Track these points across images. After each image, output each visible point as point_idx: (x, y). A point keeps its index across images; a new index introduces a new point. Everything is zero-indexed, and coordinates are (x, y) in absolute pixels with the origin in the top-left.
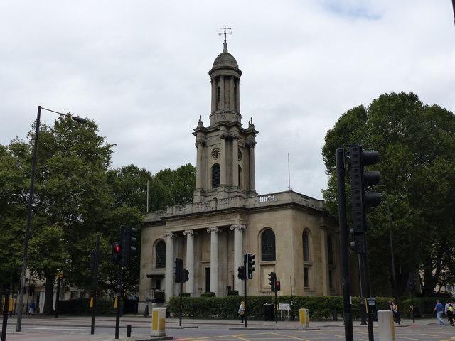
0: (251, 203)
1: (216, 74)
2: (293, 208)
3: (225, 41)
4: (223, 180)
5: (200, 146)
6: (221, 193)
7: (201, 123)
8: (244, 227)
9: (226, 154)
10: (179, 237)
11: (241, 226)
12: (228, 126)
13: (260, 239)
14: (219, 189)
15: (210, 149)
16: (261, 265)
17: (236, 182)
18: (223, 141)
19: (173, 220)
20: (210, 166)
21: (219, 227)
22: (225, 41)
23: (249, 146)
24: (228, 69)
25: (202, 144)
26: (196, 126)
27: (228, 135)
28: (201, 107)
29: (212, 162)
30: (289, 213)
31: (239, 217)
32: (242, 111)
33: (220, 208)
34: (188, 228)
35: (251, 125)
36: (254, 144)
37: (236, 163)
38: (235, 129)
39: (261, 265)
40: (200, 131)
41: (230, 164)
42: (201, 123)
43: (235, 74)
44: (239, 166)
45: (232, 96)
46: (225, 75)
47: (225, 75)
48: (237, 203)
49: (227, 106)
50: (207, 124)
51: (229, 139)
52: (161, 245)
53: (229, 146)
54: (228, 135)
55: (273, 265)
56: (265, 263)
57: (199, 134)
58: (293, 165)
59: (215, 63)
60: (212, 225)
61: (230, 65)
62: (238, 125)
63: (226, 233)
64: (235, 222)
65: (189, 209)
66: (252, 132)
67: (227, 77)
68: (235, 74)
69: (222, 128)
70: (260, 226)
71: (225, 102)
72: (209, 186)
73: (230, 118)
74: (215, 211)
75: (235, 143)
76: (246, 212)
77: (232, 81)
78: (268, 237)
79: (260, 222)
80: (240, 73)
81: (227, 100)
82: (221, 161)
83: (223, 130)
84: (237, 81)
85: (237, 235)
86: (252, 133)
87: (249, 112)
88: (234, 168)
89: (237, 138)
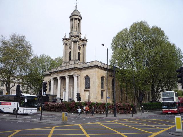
1: (72, 18)
3: (76, 6)
4: (72, 58)
5: (65, 45)
6: (72, 62)
8: (78, 75)
10: (56, 80)
13: (85, 80)
14: (70, 61)
16: (85, 91)
17: (77, 58)
18: (73, 43)
19: (53, 73)
20: (68, 52)
21: (69, 76)
22: (76, 6)
27: (75, 41)
32: (81, 32)
33: (69, 68)
36: (86, 45)
38: (78, 38)
39: (85, 91)
41: (75, 51)
43: (80, 18)
44: (79, 53)
46: (76, 18)
47: (76, 18)
50: (68, 37)
52: (50, 82)
53: (75, 45)
54: (75, 41)
55: (89, 90)
58: (99, 51)
60: (66, 75)
61: (77, 14)
63: (72, 78)
64: (75, 73)
65: (60, 69)
67: (76, 19)
68: (80, 18)
69: (73, 37)
70: (84, 75)
71: (75, 28)
72: (68, 60)
73: (75, 34)
75: (77, 43)
77: (78, 20)
78: (87, 78)
80: (81, 18)
81: (76, 27)
84: (80, 20)
85: (76, 78)
88: (77, 53)
89: (78, 42)
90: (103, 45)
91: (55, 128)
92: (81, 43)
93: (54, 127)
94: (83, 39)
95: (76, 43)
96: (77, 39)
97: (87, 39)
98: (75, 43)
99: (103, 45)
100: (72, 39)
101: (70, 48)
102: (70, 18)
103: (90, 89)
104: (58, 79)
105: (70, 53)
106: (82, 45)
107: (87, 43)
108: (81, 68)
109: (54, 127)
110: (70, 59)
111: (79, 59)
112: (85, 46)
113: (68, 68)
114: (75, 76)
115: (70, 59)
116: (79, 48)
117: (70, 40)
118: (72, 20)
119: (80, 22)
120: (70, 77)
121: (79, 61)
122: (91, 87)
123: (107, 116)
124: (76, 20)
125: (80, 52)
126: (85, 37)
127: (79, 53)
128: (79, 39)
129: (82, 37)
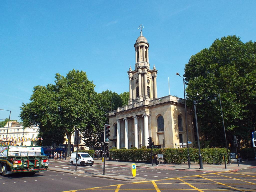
1: (137, 46)
10: (122, 121)
17: (146, 94)
37: (147, 85)
39: (158, 134)
43: (147, 46)
44: (148, 87)
53: (143, 78)
55: (163, 133)
56: (159, 132)
60: (134, 115)
67: (142, 47)
68: (147, 46)
70: (156, 114)
77: (144, 48)
90: (178, 74)
91: (121, 187)
93: (119, 186)
95: (144, 75)
99: (178, 74)
102: (135, 46)
103: (165, 132)
108: (152, 106)
109: (119, 186)
111: (149, 95)
122: (166, 128)
123: (189, 167)
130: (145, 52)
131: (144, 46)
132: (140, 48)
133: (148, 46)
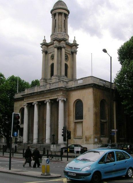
0: (72, 85)
1: (54, 12)
2: (92, 87)
4: (55, 73)
5: (44, 53)
6: (54, 79)
7: (45, 40)
8: (65, 99)
9: (58, 57)
10: (31, 106)
11: (62, 99)
12: (59, 41)
14: (53, 78)
15: (50, 55)
17: (63, 73)
18: (56, 50)
20: (50, 64)
23: (74, 53)
24: (60, 9)
25: (45, 52)
26: (42, 42)
28: (46, 33)
29: (51, 62)
30: (90, 91)
31: (61, 93)
34: (35, 101)
35: (75, 41)
36: (76, 52)
37: (64, 62)
38: (63, 42)
40: (45, 45)
42: (45, 40)
45: (63, 25)
48: (61, 85)
49: (60, 30)
50: (49, 41)
51: (59, 48)
52: (22, 110)
53: (59, 52)
55: (82, 122)
57: (44, 46)
59: (55, 6)
61: (61, 7)
62: (65, 40)
63: (55, 103)
66: (75, 45)
67: (60, 14)
69: (55, 42)
73: (60, 37)
74: (49, 90)
75: (63, 50)
76: (67, 91)
77: (63, 15)
78: (79, 104)
79: (75, 96)
82: (55, 61)
83: (56, 43)
84: (66, 16)
85: (61, 105)
86: (75, 45)
87: (74, 34)
89: (64, 48)
92: (69, 49)
94: (72, 44)
96: (63, 44)
97: (77, 43)
98: (59, 50)
100: (55, 45)
101: (52, 57)
102: (51, 13)
103: (84, 120)
104: (34, 105)
105: (52, 65)
106: (70, 53)
107: (77, 50)
110: (52, 74)
111: (66, 74)
112: (74, 54)
113: (49, 89)
114: (60, 102)
115: (52, 74)
116: (67, 58)
117: (52, 46)
118: (54, 15)
119: (67, 18)
120: (53, 102)
121: (65, 78)
124: (60, 16)
125: (68, 63)
126: (75, 41)
127: (66, 66)
128: (66, 44)
129: (71, 41)
130: (64, 20)
131: (63, 13)
132: (57, 15)
133: (67, 13)
